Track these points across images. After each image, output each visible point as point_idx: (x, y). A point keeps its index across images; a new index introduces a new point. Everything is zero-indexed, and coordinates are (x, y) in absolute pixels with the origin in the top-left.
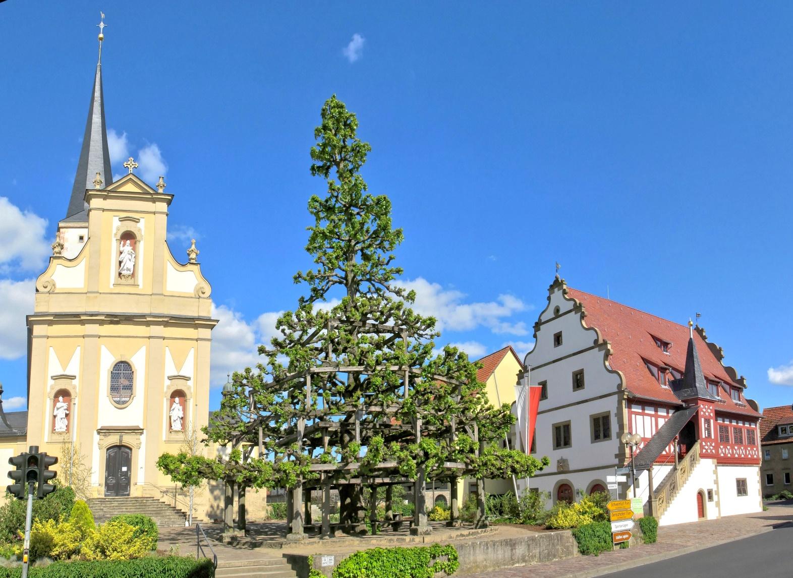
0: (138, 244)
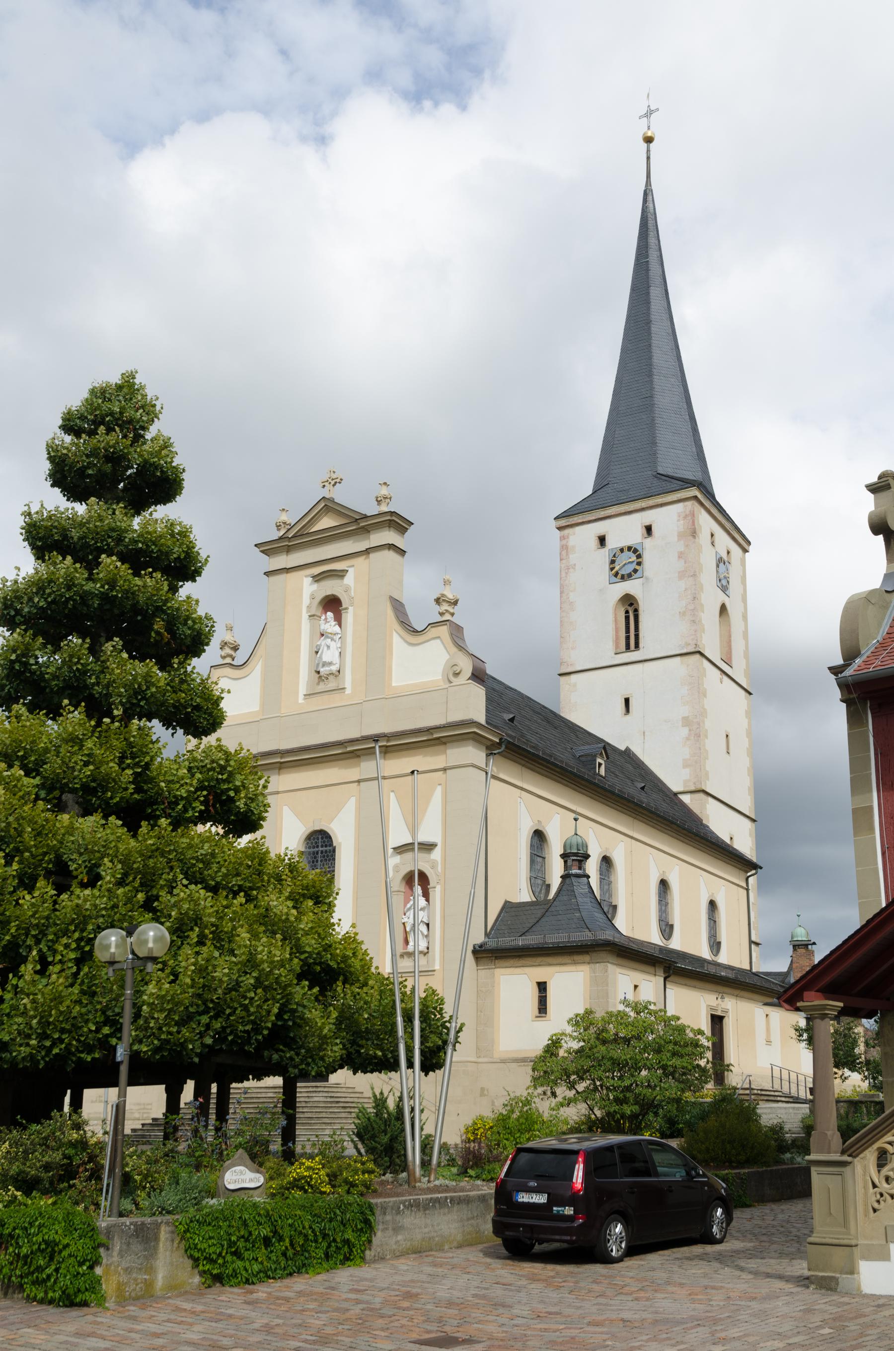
0: (344, 615)
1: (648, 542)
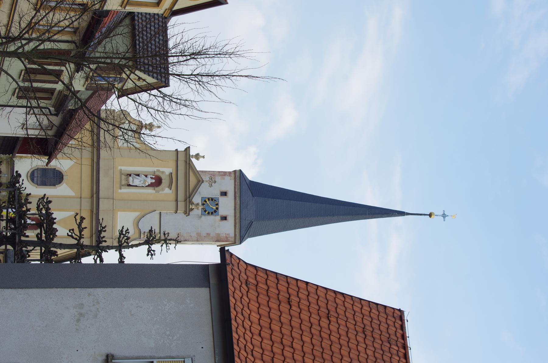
0: (152, 188)
1: (218, 218)
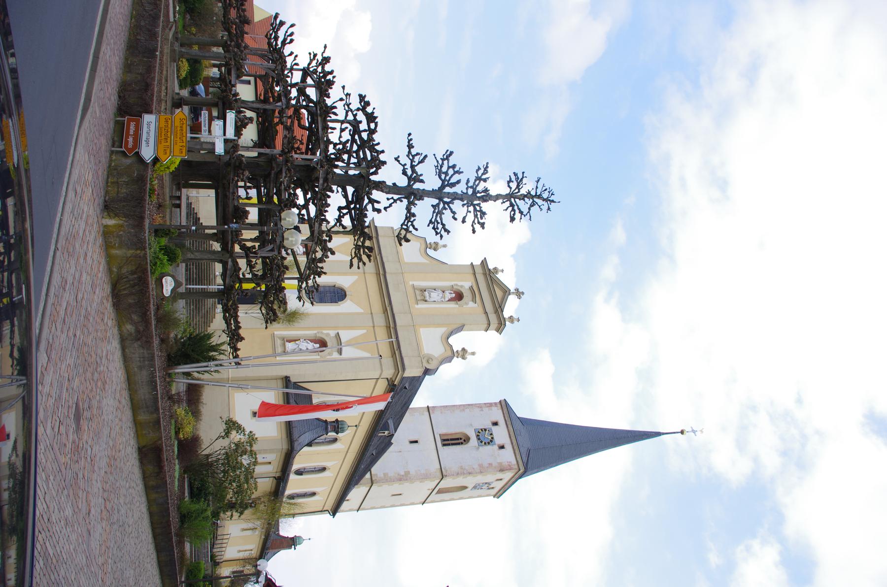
1: (496, 447)
